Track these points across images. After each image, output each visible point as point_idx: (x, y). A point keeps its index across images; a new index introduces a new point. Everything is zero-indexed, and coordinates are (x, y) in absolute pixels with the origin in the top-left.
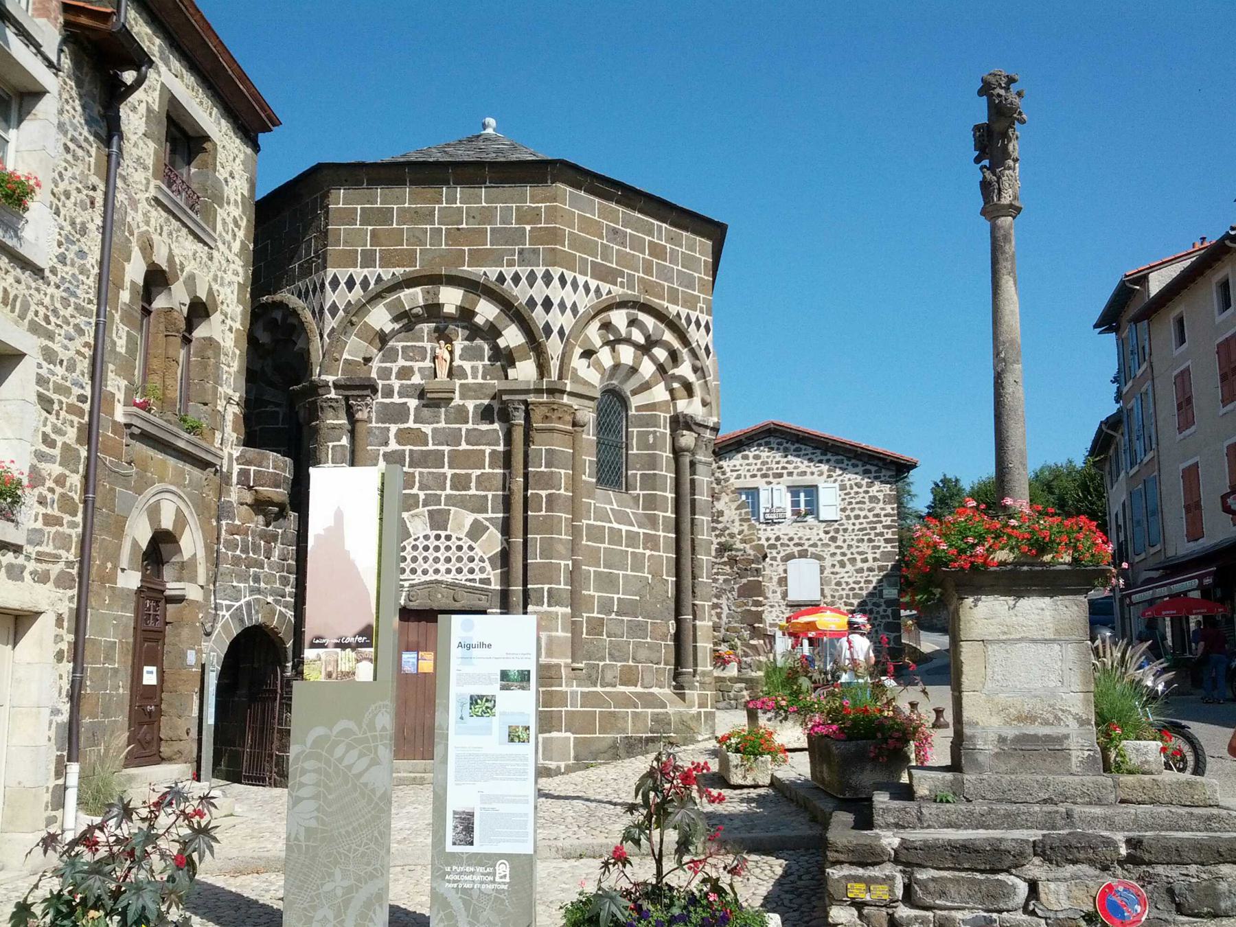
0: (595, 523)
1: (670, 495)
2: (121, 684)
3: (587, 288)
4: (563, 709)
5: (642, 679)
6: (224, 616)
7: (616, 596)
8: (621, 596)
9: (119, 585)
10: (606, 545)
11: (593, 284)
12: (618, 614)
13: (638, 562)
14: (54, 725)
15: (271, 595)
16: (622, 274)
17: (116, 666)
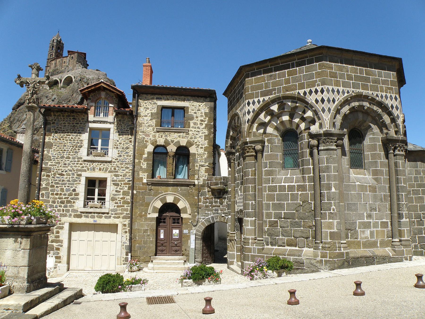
0: (272, 185)
1: (311, 167)
2: (151, 238)
3: (259, 102)
4: (250, 254)
5: (298, 244)
6: (201, 221)
7: (283, 212)
8: (285, 211)
9: (148, 217)
10: (278, 192)
11: (261, 99)
12: (284, 218)
13: (295, 198)
14: (124, 245)
15: (223, 214)
16: (275, 90)
17: (149, 234)
